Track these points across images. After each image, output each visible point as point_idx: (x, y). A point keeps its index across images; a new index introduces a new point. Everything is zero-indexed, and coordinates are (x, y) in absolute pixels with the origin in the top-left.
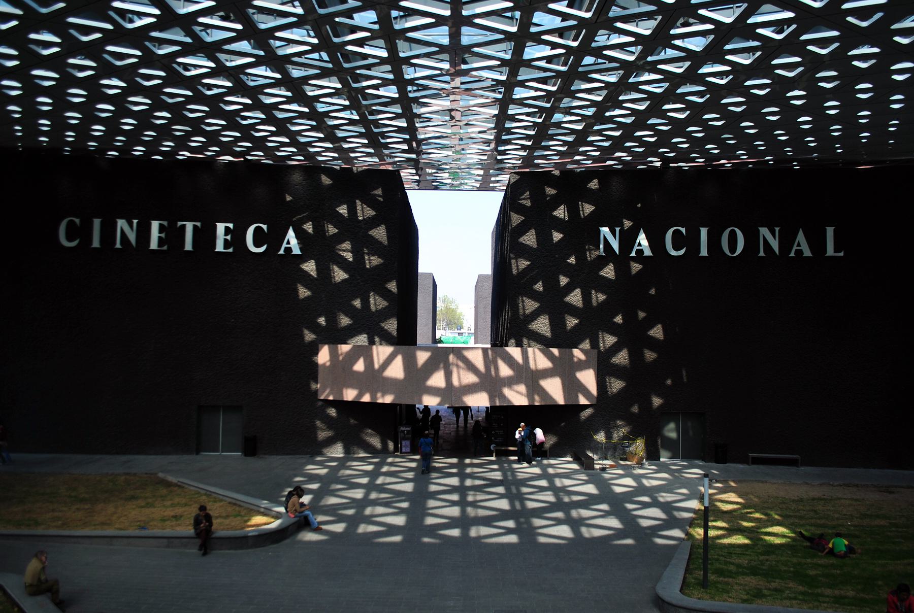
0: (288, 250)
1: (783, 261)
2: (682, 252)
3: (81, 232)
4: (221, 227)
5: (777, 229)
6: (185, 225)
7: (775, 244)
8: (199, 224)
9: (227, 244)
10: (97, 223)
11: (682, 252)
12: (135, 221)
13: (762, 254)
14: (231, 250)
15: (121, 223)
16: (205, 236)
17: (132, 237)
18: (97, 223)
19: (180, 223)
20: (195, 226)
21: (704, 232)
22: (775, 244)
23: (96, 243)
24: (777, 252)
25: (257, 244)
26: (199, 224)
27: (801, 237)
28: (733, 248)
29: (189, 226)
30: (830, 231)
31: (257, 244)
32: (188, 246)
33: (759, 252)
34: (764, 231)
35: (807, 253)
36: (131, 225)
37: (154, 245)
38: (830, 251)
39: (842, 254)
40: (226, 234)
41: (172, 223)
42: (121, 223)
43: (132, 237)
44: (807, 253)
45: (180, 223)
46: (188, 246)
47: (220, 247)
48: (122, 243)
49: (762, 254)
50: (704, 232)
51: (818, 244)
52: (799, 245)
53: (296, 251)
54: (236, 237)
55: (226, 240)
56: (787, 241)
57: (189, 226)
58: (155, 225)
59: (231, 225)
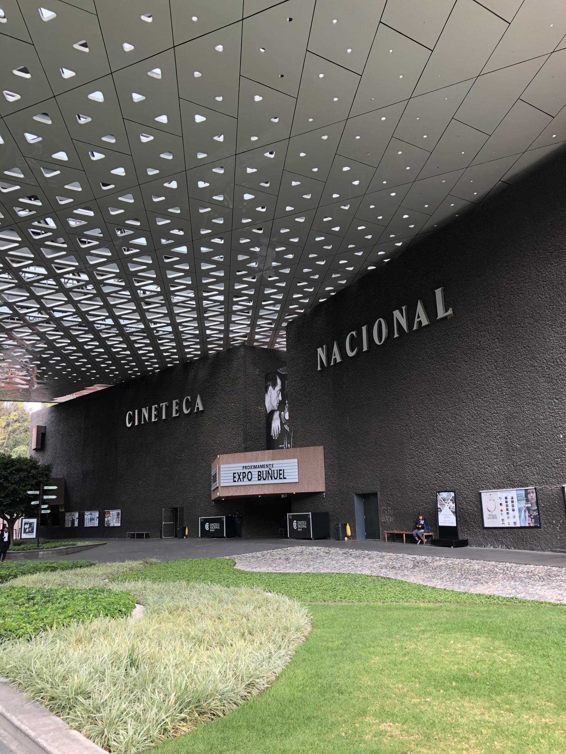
1: (413, 335)
4: (174, 402)
10: (136, 411)
15: (144, 410)
21: (364, 329)
30: (439, 293)
34: (396, 313)
37: (153, 420)
38: (441, 313)
41: (159, 406)
49: (396, 335)
51: (431, 311)
53: (201, 409)
58: (153, 407)
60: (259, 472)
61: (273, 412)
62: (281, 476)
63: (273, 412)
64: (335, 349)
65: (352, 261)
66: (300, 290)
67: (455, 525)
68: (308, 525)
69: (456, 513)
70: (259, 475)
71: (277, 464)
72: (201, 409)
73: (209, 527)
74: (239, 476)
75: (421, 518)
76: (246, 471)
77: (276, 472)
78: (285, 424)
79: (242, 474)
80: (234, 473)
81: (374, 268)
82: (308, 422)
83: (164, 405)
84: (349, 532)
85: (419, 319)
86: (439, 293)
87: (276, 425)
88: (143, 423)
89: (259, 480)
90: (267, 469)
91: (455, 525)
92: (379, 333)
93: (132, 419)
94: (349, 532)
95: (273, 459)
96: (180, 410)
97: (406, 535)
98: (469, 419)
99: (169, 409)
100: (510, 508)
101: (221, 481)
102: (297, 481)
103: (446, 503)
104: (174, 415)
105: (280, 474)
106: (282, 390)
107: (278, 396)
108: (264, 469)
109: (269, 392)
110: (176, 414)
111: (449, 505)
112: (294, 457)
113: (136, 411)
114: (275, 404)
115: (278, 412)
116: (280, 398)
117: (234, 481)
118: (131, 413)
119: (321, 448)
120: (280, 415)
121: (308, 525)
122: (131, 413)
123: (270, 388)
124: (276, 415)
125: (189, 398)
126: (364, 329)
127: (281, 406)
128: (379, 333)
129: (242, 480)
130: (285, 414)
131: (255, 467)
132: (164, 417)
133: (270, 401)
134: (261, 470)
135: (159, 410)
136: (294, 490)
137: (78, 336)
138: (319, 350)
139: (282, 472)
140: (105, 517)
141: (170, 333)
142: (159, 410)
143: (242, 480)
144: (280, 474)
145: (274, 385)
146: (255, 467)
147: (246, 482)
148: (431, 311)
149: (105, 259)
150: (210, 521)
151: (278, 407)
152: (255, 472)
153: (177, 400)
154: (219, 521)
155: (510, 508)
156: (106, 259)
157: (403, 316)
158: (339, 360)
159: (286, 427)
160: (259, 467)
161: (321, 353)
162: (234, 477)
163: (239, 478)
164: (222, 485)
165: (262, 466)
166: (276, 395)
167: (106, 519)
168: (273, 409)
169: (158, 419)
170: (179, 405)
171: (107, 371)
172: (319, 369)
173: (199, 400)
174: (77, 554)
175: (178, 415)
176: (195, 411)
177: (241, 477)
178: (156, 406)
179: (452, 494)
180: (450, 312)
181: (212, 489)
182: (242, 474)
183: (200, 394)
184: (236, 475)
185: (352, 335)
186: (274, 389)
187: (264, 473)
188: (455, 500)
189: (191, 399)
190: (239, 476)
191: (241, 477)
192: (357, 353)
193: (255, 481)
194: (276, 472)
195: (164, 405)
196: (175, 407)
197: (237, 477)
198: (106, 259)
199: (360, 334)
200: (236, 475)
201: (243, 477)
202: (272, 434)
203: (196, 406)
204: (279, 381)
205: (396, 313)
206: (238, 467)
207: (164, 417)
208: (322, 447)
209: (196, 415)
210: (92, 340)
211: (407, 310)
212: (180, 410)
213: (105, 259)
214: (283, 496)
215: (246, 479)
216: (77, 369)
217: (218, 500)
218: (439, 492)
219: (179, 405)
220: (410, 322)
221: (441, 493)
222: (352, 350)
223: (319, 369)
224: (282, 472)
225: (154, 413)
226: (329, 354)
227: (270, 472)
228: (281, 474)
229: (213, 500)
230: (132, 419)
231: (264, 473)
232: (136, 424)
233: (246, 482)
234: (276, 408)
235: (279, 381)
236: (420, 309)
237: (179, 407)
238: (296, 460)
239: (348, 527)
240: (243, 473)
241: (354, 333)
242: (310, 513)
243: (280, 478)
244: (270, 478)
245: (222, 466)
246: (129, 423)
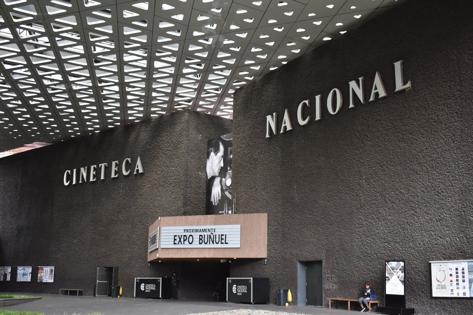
4: (114, 163)
5: (360, 79)
10: (75, 170)
15: (82, 169)
21: (318, 98)
30: (398, 66)
34: (353, 84)
37: (91, 180)
38: (399, 86)
41: (98, 166)
49: (351, 106)
51: (389, 83)
53: (141, 171)
55: (115, 170)
58: (92, 167)
60: (200, 236)
61: (213, 178)
62: (223, 241)
63: (213, 178)
64: (286, 117)
65: (310, 30)
66: (253, 56)
67: (403, 294)
68: (249, 290)
69: (404, 282)
70: (200, 239)
71: (220, 229)
72: (141, 171)
73: (145, 288)
74: (180, 239)
75: (368, 287)
76: (188, 234)
77: (217, 237)
78: (226, 190)
80: (175, 236)
81: (330, 39)
82: (252, 189)
83: (103, 165)
84: (290, 298)
85: (376, 91)
86: (398, 66)
87: (216, 191)
88: (80, 182)
89: (200, 243)
90: (209, 234)
91: (403, 294)
92: (333, 102)
93: (70, 178)
94: (290, 298)
95: (215, 224)
96: (119, 172)
97: (351, 302)
98: (423, 191)
99: (108, 170)
100: (460, 279)
101: (162, 243)
102: (239, 246)
103: (395, 272)
104: (113, 176)
105: (222, 239)
106: (225, 157)
107: (220, 162)
108: (206, 234)
109: (210, 158)
110: (115, 175)
111: (398, 274)
112: (236, 223)
113: (75, 170)
115: (219, 178)
116: (222, 164)
117: (175, 244)
118: (69, 171)
120: (221, 181)
121: (249, 290)
122: (69, 171)
123: (212, 154)
124: (217, 181)
125: (129, 159)
126: (318, 98)
127: (223, 172)
128: (333, 102)
129: (183, 243)
130: (226, 180)
131: (197, 231)
132: (102, 178)
133: (212, 167)
134: (202, 234)
135: (98, 170)
136: (235, 255)
137: (25, 90)
138: (269, 118)
139: (223, 237)
140: (38, 273)
141: (117, 93)
142: (98, 170)
143: (183, 243)
144: (222, 239)
145: (217, 151)
146: (197, 231)
147: (187, 245)
148: (389, 83)
149: (65, 11)
150: (147, 282)
151: (220, 173)
152: (196, 236)
153: (117, 162)
154: (155, 282)
155: (460, 279)
156: (65, 11)
157: (352, 89)
158: (289, 128)
159: (227, 193)
160: (200, 231)
161: (271, 121)
162: (175, 240)
163: (180, 240)
164: (162, 247)
165: (204, 230)
166: (217, 161)
167: (39, 275)
168: (214, 175)
169: (97, 179)
170: (119, 166)
171: (48, 128)
172: (267, 136)
173: (139, 163)
174: (31, 302)
175: (117, 176)
176: (135, 173)
177: (182, 240)
178: (95, 166)
179: (402, 264)
180: (408, 85)
181: (149, 251)
183: (140, 156)
184: (177, 238)
185: (305, 104)
186: (216, 155)
187: (206, 237)
188: (404, 270)
189: (132, 160)
190: (180, 239)
191: (182, 240)
192: (309, 122)
193: (196, 244)
194: (217, 237)
195: (103, 165)
196: (114, 168)
197: (178, 240)
198: (65, 11)
199: (313, 103)
200: (177, 238)
201: (184, 240)
202: (212, 199)
203: (136, 168)
204: (222, 148)
205: (353, 84)
207: (102, 178)
210: (39, 95)
211: (364, 82)
212: (119, 172)
213: (65, 11)
214: (222, 261)
215: (186, 242)
216: (18, 125)
217: (155, 263)
218: (388, 261)
219: (119, 166)
220: (367, 93)
221: (390, 263)
222: (304, 119)
223: (267, 136)
224: (223, 237)
225: (92, 173)
226: (279, 122)
227: (212, 236)
228: (222, 239)
229: (150, 262)
230: (70, 178)
231: (206, 237)
232: (74, 183)
233: (187, 245)
234: (217, 174)
235: (222, 148)
236: (377, 81)
237: (118, 169)
238: (239, 226)
239: (289, 294)
240: (184, 236)
241: (307, 102)
242: (252, 278)
243: (222, 243)
244: (211, 242)
245: (163, 228)
246: (67, 182)
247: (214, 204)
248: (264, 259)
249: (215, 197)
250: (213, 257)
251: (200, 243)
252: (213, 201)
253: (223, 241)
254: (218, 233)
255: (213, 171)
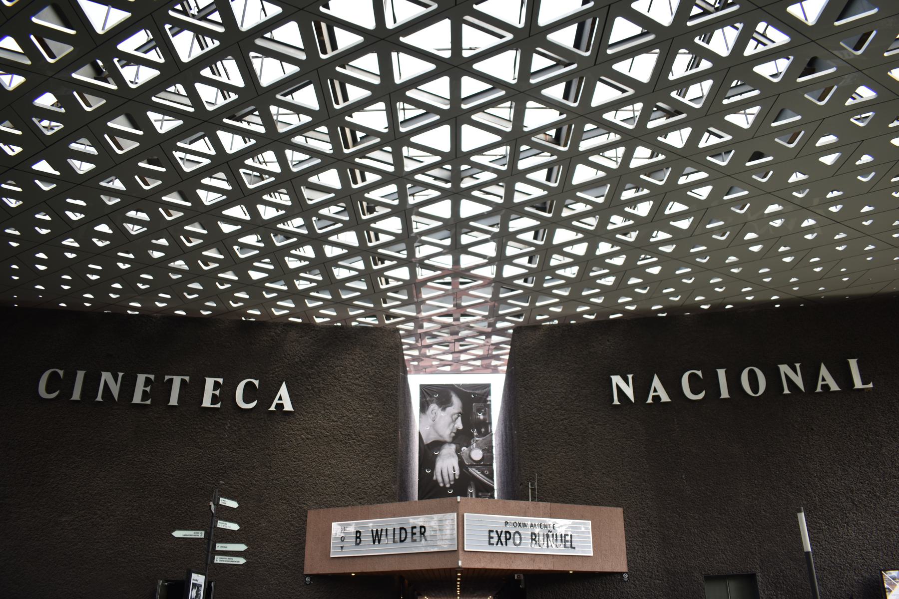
0: (280, 406)
2: (701, 396)
3: (61, 385)
4: (210, 382)
5: (798, 365)
6: (172, 379)
7: (799, 381)
8: (187, 378)
9: (214, 399)
10: (80, 375)
11: (701, 396)
12: (121, 374)
13: (786, 391)
14: (218, 406)
15: (106, 376)
16: (192, 391)
17: (115, 389)
18: (80, 375)
19: (167, 377)
20: (183, 381)
21: (721, 373)
22: (799, 381)
23: (76, 395)
24: (803, 389)
25: (246, 400)
26: (187, 378)
27: (824, 371)
28: (755, 388)
29: (177, 381)
30: (853, 364)
31: (246, 400)
32: (174, 401)
33: (783, 390)
34: (784, 369)
35: (834, 387)
36: (116, 378)
37: (137, 399)
38: (858, 384)
39: (871, 385)
40: (215, 389)
41: (160, 378)
42: (106, 376)
43: (115, 389)
44: (834, 387)
45: (167, 377)
46: (174, 401)
47: (207, 402)
48: (118, 375)
49: (786, 391)
50: (721, 373)
52: (824, 380)
53: (288, 407)
54: (226, 394)
56: (811, 377)
57: (177, 381)
58: (141, 378)
59: (221, 380)
61: (438, 445)
79: (503, 535)
80: (490, 531)
86: (853, 364)
92: (754, 382)
107: (454, 421)
114: (446, 433)
115: (453, 447)
119: (620, 511)
120: (458, 451)
124: (449, 450)
128: (754, 382)
130: (470, 451)
144: (566, 541)
152: (526, 533)
162: (490, 538)
168: (441, 439)
182: (503, 535)
184: (494, 535)
200: (494, 535)
201: (507, 539)
206: (498, 521)
208: (620, 511)
209: (266, 417)
223: (616, 402)
224: (568, 538)
226: (642, 388)
233: (510, 548)
234: (448, 439)
240: (506, 532)
247: (442, 485)
248: (621, 573)
249: (445, 475)
250: (561, 569)
251: (357, 544)
252: (440, 479)
253: (568, 544)
254: (560, 531)
255: (437, 432)
